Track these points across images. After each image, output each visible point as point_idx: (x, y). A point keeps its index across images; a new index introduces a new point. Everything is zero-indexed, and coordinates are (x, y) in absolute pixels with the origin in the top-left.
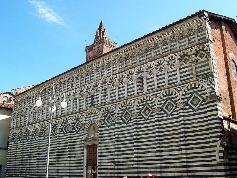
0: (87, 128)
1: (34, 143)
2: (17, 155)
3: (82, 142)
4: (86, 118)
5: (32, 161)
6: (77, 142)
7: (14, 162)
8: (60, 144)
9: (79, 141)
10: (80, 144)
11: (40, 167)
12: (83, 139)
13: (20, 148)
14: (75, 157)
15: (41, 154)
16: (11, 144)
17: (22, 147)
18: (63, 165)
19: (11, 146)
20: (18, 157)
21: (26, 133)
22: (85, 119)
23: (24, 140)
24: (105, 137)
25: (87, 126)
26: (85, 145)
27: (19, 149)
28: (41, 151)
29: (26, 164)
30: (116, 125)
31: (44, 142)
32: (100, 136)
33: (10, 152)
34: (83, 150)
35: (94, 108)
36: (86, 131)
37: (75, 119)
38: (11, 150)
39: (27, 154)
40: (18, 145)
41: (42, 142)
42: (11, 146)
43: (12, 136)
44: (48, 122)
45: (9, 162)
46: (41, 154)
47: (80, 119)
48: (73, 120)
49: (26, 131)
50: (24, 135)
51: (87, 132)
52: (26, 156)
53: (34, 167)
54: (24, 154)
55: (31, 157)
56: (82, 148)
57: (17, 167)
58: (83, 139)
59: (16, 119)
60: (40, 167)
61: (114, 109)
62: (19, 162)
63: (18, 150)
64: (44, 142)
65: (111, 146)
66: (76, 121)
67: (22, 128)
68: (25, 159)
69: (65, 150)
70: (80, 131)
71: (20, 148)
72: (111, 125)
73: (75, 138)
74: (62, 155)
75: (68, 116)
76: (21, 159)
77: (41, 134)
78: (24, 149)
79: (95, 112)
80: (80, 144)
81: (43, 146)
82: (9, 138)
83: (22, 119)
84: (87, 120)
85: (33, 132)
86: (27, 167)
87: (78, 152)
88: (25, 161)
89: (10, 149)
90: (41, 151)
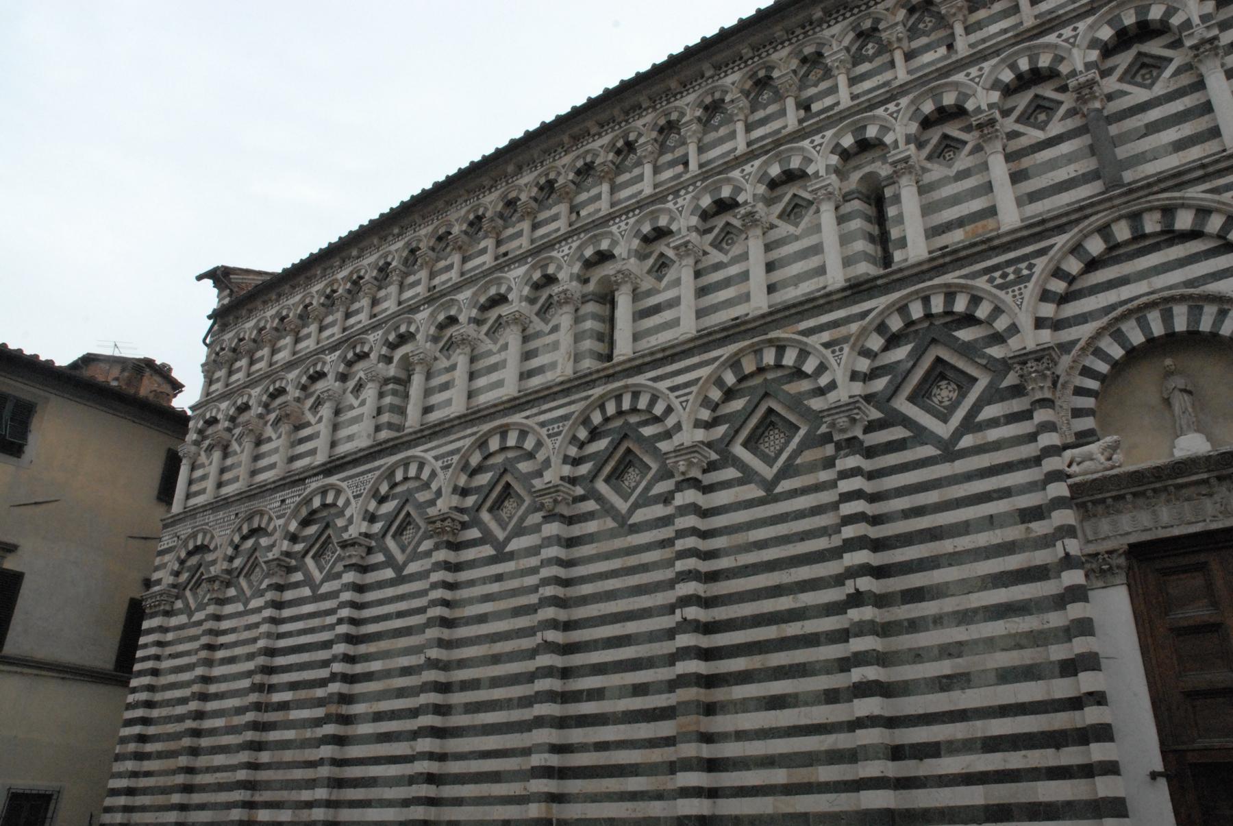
0: (1079, 391)
1: (381, 602)
2: (211, 706)
3: (1064, 517)
4: (1064, 299)
5: (354, 752)
7: (183, 761)
8: (713, 577)
9: (991, 522)
10: (1008, 548)
11: (458, 802)
12: (1059, 489)
13: (238, 651)
14: (945, 684)
15: (474, 685)
16: (163, 630)
17: (261, 643)
18: (779, 776)
19: (159, 644)
20: (219, 723)
21: (304, 539)
22: (1048, 310)
23: (280, 588)
25: (1087, 372)
26: (1091, 549)
27: (231, 660)
28: (462, 664)
29: (298, 774)
31: (495, 588)
33: (151, 688)
36: (1077, 413)
37: (893, 341)
38: (155, 672)
39: (302, 694)
40: (224, 632)
41: (471, 583)
42: (159, 644)
43: (177, 574)
44: (542, 418)
45: (130, 765)
46: (474, 685)
48: (876, 342)
49: (305, 523)
50: (288, 554)
51: (1088, 423)
52: (295, 714)
53: (389, 804)
54: (277, 697)
55: (347, 720)
57: (202, 807)
58: (1059, 489)
59: (217, 455)
60: (458, 802)
62: (219, 760)
63: (217, 671)
64: (495, 588)
66: (917, 356)
67: (271, 504)
68: (289, 735)
69: (793, 629)
70: (994, 423)
71: (238, 651)
73: (932, 497)
74: (745, 677)
75: (804, 325)
76: (249, 735)
77: (464, 526)
78: (280, 661)
80: (1008, 548)
81: (482, 619)
82: (148, 584)
83: (265, 448)
84: (1083, 319)
85: (372, 518)
86: (309, 805)
87: (997, 628)
88: (288, 755)
89: (149, 664)
90: (462, 664)
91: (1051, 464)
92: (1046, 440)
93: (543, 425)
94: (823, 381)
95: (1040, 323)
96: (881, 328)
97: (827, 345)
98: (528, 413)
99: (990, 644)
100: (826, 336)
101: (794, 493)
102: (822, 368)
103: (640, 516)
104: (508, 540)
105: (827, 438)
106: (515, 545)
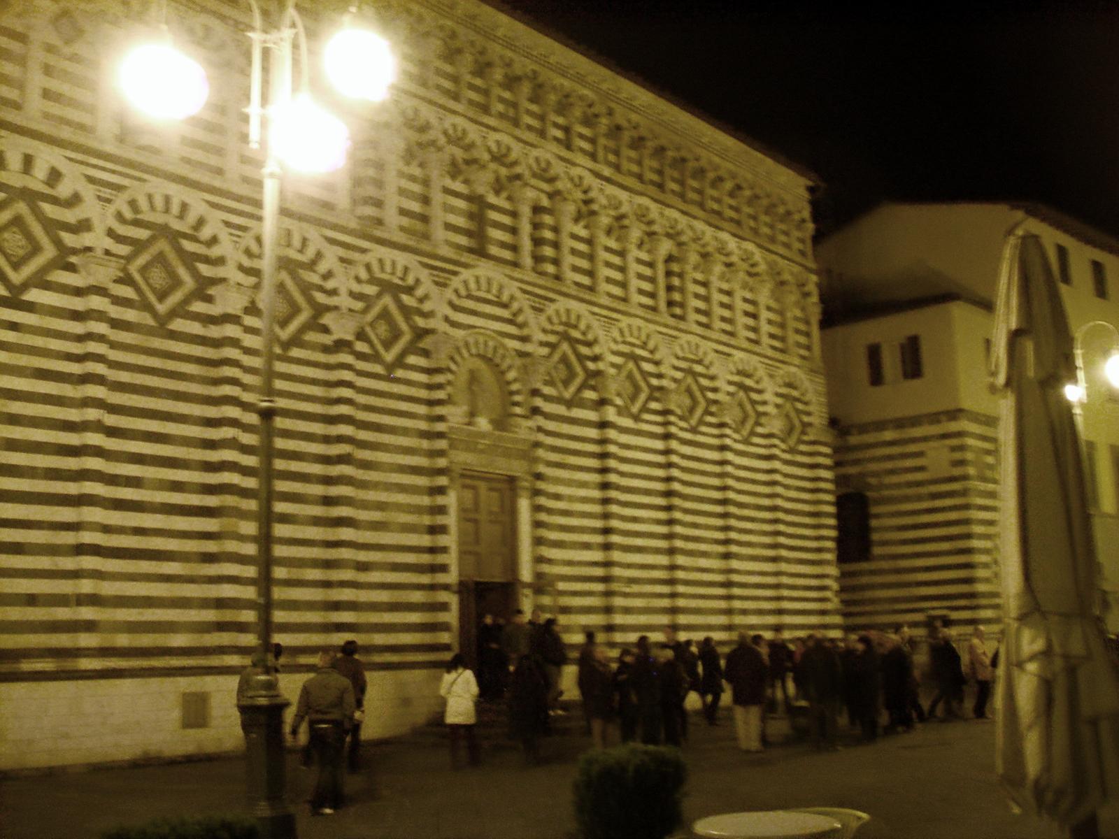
6: (392, 430)
9: (405, 432)
12: (440, 427)
24: (555, 449)
30: (611, 414)
32: (541, 437)
34: (441, 491)
35: (512, 278)
47: (410, 290)
48: (364, 275)
56: (442, 481)
58: (440, 427)
61: (602, 338)
65: (585, 500)
66: (379, 295)
72: (582, 404)
79: (505, 298)
91: (439, 410)
92: (440, 395)
93: (91, 180)
94: (330, 285)
95: (447, 319)
96: (368, 267)
97: (342, 260)
98: (73, 155)
99: (399, 507)
100: (342, 252)
101: (299, 361)
102: (328, 276)
103: (178, 325)
104: (25, 286)
105: (326, 330)
106: (34, 295)
